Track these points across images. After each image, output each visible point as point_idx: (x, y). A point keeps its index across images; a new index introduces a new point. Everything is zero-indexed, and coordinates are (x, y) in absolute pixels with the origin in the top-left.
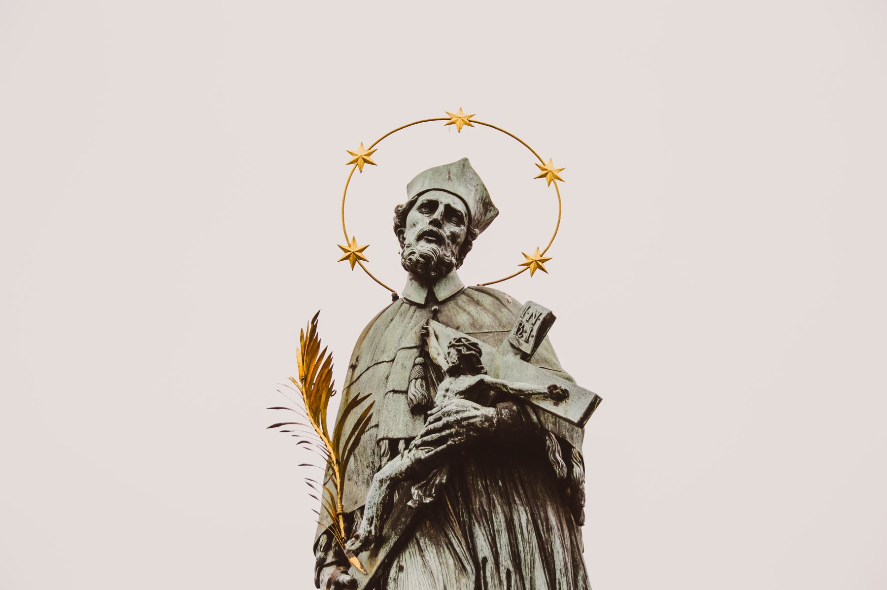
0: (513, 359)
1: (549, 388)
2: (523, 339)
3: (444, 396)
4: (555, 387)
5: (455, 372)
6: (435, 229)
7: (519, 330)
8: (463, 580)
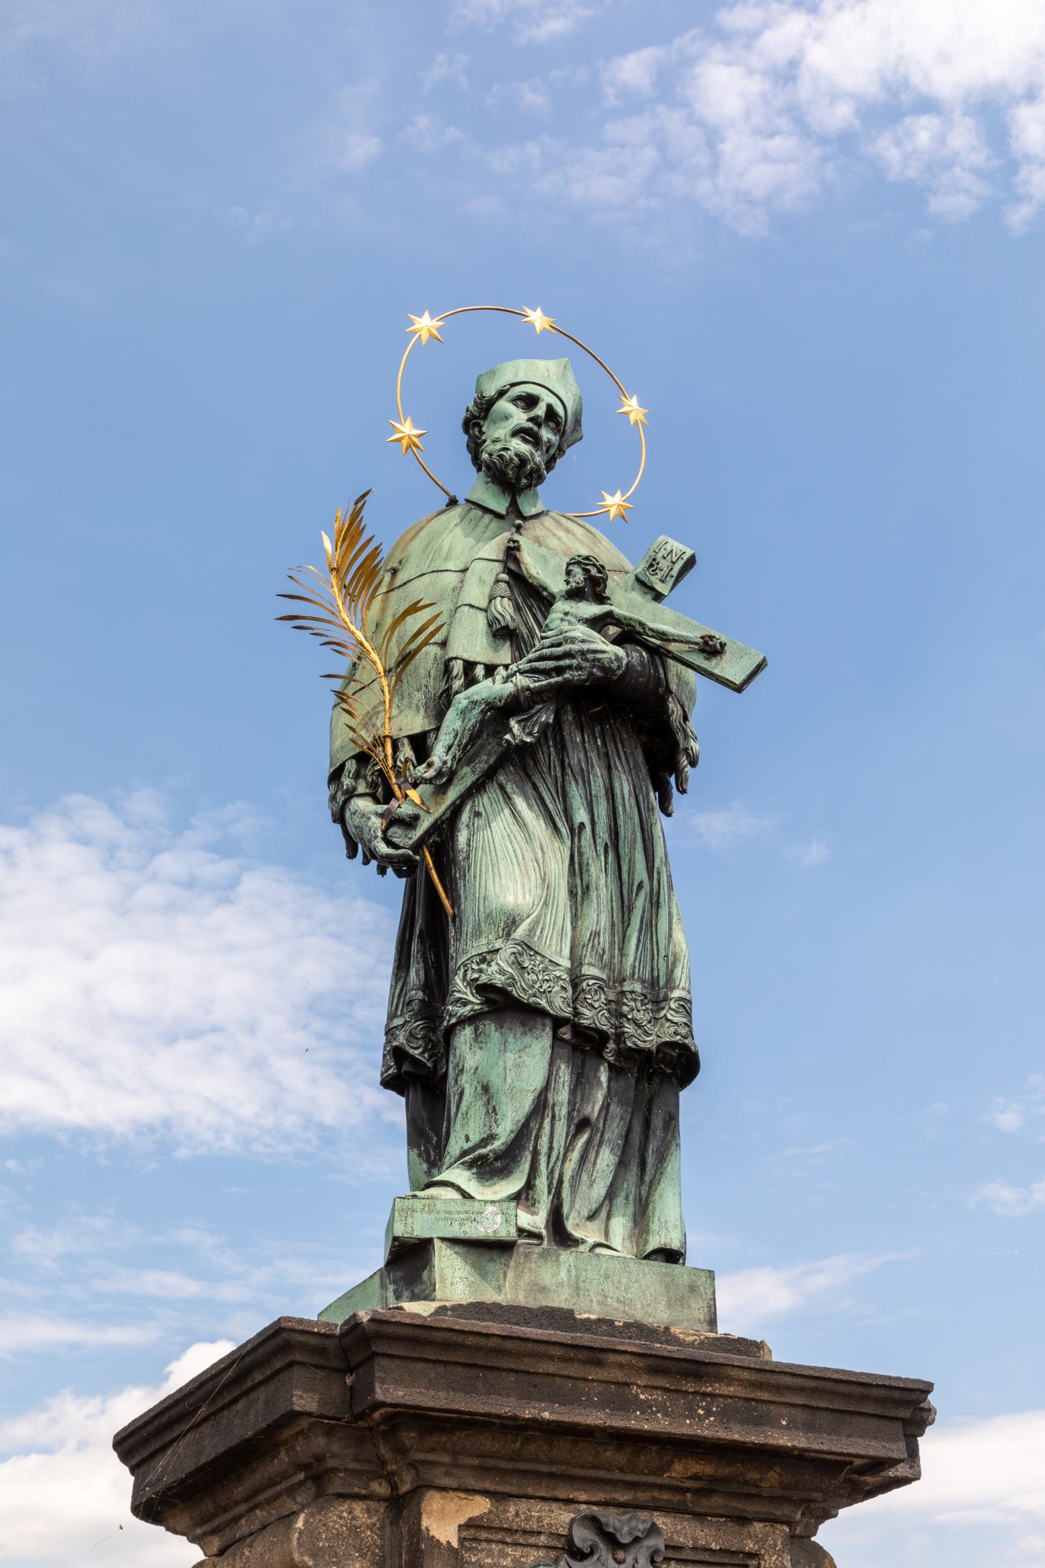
0: (637, 596)
1: (702, 638)
2: (659, 576)
3: (562, 620)
4: (711, 637)
5: (574, 594)
6: (535, 428)
7: (651, 565)
8: (556, 844)
